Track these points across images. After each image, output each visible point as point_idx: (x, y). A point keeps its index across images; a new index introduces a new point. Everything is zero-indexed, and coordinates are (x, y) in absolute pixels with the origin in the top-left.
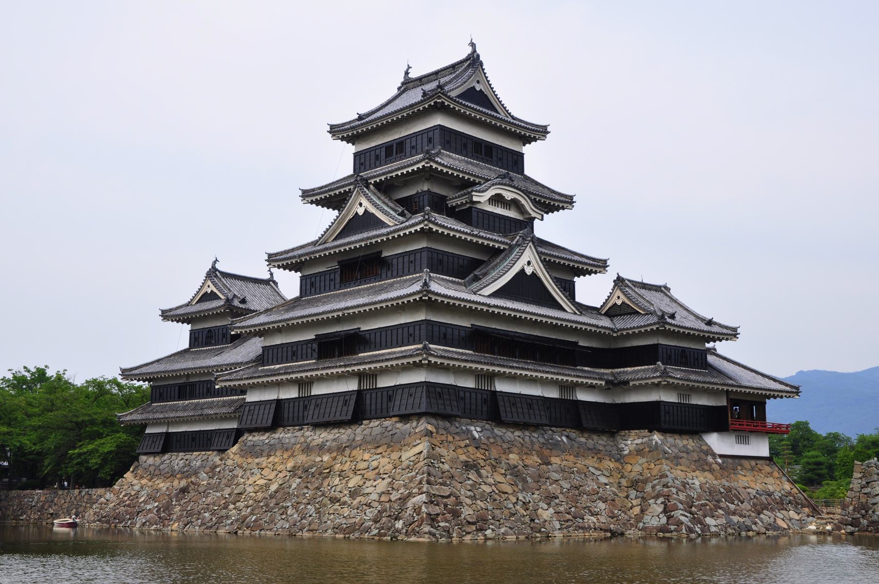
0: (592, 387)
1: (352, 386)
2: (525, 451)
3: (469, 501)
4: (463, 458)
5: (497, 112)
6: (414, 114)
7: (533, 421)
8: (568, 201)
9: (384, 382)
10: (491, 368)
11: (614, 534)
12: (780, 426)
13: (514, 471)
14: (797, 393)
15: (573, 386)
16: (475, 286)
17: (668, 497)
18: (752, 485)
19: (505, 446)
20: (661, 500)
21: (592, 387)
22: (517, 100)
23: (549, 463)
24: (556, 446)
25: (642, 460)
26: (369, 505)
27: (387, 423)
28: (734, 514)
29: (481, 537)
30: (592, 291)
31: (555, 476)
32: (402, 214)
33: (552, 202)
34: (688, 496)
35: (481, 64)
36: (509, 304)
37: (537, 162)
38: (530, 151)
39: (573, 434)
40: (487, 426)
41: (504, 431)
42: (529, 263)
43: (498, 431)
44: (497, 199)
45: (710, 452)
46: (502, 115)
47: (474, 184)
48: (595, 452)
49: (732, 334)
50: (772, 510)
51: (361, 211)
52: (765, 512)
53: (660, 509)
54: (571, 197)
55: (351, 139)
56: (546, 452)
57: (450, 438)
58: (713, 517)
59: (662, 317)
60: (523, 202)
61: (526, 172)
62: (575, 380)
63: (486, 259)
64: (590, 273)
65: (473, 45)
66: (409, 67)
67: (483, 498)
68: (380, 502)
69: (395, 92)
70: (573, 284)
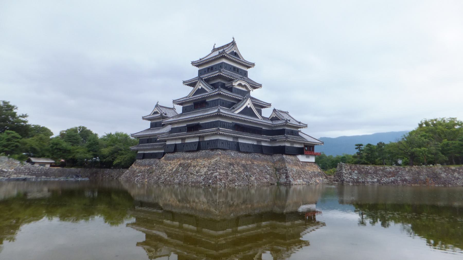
0: (266, 141)
1: (197, 140)
2: (247, 160)
4: (229, 162)
6: (216, 59)
7: (249, 151)
8: (260, 86)
9: (206, 139)
10: (237, 135)
11: (271, 184)
13: (244, 166)
16: (233, 110)
17: (287, 173)
19: (241, 158)
20: (285, 174)
21: (266, 141)
22: (246, 56)
24: (255, 158)
25: (280, 163)
26: (202, 175)
27: (207, 151)
30: (267, 113)
31: (255, 167)
32: (212, 89)
33: (255, 86)
34: (292, 173)
37: (252, 74)
38: (249, 71)
43: (239, 154)
44: (240, 85)
45: (299, 161)
46: (242, 60)
47: (233, 80)
48: (266, 160)
49: (306, 126)
50: (315, 177)
51: (200, 88)
53: (284, 177)
56: (253, 160)
59: (286, 121)
63: (236, 102)
64: (266, 107)
65: (233, 38)
66: (215, 44)
67: (235, 173)
68: (205, 174)
69: (211, 52)
70: (261, 110)
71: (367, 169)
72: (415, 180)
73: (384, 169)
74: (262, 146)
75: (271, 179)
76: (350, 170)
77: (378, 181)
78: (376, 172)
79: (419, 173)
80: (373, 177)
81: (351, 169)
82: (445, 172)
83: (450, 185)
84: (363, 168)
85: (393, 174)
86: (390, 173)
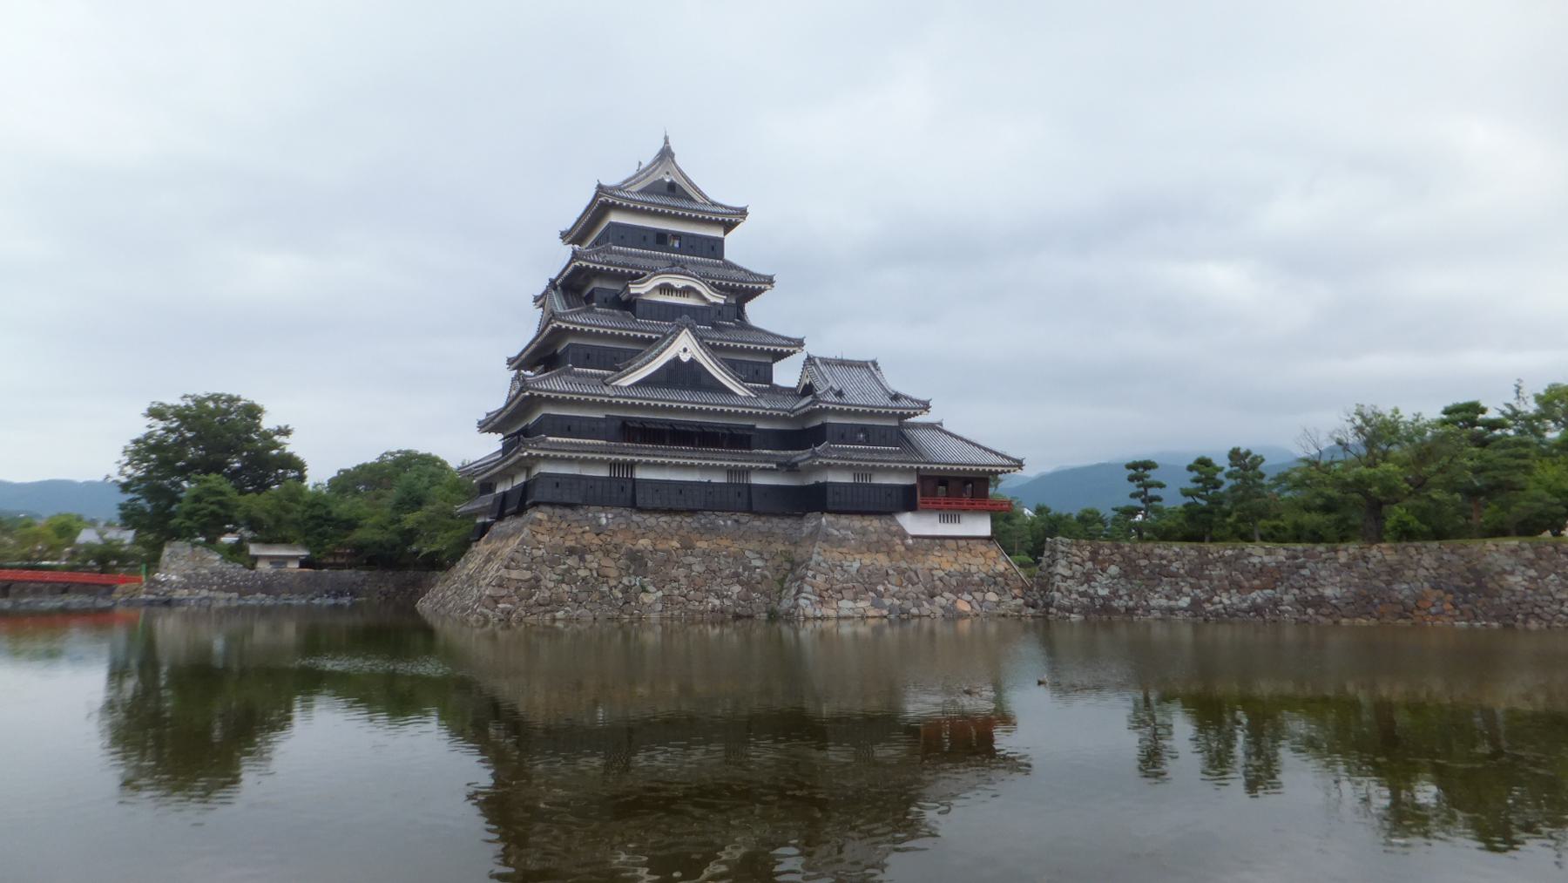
3: (551, 585)
4: (573, 544)
5: (691, 199)
11: (737, 617)
15: (748, 471)
22: (717, 188)
23: (692, 547)
24: (714, 530)
29: (548, 617)
30: (786, 374)
35: (672, 155)
36: (649, 393)
37: (738, 248)
39: (744, 518)
44: (666, 289)
52: (946, 594)
57: (564, 525)
58: (855, 600)
60: (699, 288)
71: (1162, 557)
72: (1363, 603)
73: (1237, 558)
74: (750, 486)
75: (747, 599)
76: (1089, 565)
77: (1196, 604)
79: (1394, 572)
80: (1179, 592)
81: (1093, 559)
82: (1530, 564)
83: (1533, 624)
84: (1147, 556)
85: (1270, 577)
86: (1262, 570)
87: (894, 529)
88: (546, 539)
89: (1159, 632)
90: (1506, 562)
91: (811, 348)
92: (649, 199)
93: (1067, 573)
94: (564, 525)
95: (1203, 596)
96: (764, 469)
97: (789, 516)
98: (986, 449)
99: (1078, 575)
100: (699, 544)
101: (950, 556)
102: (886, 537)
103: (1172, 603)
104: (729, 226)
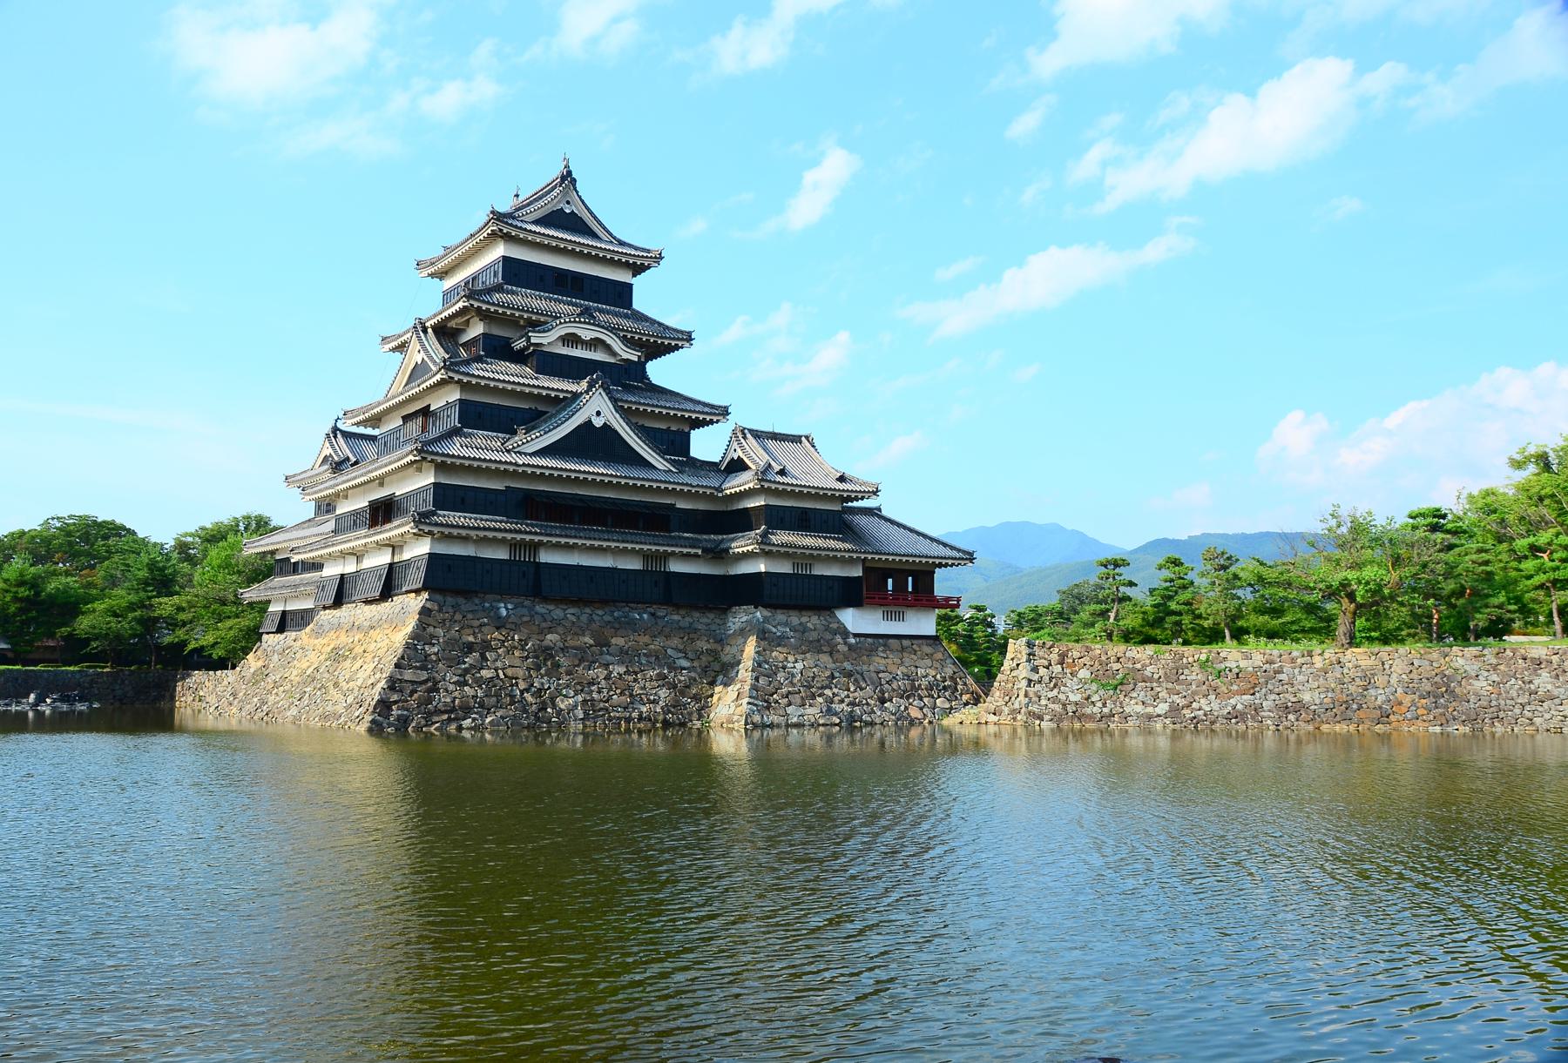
3: (451, 687)
5: (595, 236)
8: (688, 337)
11: (667, 724)
12: (948, 599)
14: (971, 560)
15: (666, 556)
18: (892, 668)
21: (696, 556)
23: (608, 645)
28: (842, 701)
30: (707, 444)
35: (574, 181)
40: (527, 603)
41: (551, 607)
42: (598, 414)
54: (689, 333)
55: (442, 275)
56: (608, 632)
57: (458, 617)
60: (609, 341)
61: (635, 306)
62: (654, 548)
64: (711, 422)
77: (1175, 710)
78: (1175, 674)
87: (834, 626)
88: (440, 632)
89: (1135, 742)
90: (1472, 668)
91: (738, 418)
92: (543, 230)
93: (1035, 677)
94: (458, 617)
95: (1182, 702)
96: (688, 555)
97: (710, 610)
98: (932, 539)
99: (1046, 679)
100: (614, 641)
101: (894, 658)
102: (828, 636)
103: (1150, 710)
104: (638, 269)
